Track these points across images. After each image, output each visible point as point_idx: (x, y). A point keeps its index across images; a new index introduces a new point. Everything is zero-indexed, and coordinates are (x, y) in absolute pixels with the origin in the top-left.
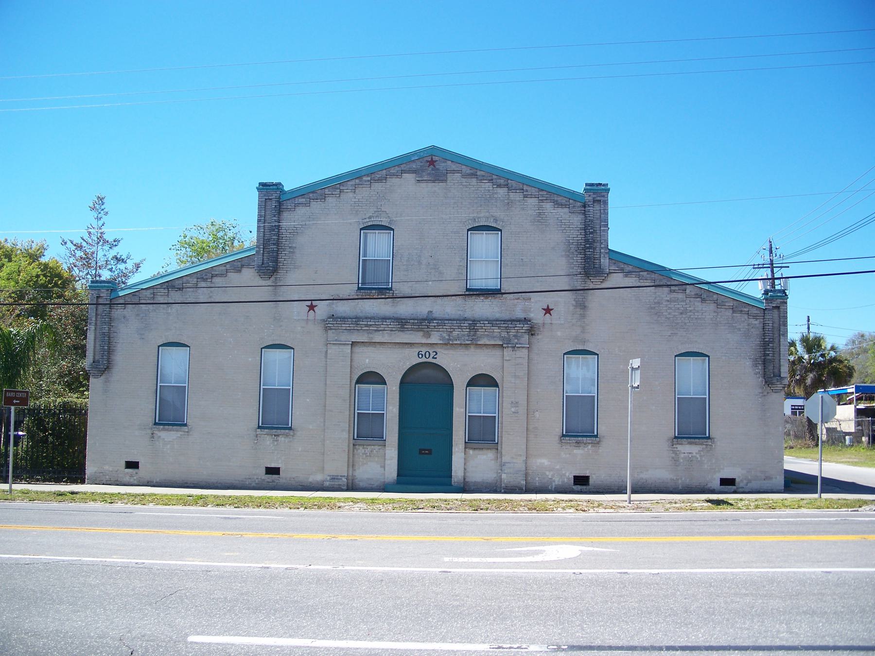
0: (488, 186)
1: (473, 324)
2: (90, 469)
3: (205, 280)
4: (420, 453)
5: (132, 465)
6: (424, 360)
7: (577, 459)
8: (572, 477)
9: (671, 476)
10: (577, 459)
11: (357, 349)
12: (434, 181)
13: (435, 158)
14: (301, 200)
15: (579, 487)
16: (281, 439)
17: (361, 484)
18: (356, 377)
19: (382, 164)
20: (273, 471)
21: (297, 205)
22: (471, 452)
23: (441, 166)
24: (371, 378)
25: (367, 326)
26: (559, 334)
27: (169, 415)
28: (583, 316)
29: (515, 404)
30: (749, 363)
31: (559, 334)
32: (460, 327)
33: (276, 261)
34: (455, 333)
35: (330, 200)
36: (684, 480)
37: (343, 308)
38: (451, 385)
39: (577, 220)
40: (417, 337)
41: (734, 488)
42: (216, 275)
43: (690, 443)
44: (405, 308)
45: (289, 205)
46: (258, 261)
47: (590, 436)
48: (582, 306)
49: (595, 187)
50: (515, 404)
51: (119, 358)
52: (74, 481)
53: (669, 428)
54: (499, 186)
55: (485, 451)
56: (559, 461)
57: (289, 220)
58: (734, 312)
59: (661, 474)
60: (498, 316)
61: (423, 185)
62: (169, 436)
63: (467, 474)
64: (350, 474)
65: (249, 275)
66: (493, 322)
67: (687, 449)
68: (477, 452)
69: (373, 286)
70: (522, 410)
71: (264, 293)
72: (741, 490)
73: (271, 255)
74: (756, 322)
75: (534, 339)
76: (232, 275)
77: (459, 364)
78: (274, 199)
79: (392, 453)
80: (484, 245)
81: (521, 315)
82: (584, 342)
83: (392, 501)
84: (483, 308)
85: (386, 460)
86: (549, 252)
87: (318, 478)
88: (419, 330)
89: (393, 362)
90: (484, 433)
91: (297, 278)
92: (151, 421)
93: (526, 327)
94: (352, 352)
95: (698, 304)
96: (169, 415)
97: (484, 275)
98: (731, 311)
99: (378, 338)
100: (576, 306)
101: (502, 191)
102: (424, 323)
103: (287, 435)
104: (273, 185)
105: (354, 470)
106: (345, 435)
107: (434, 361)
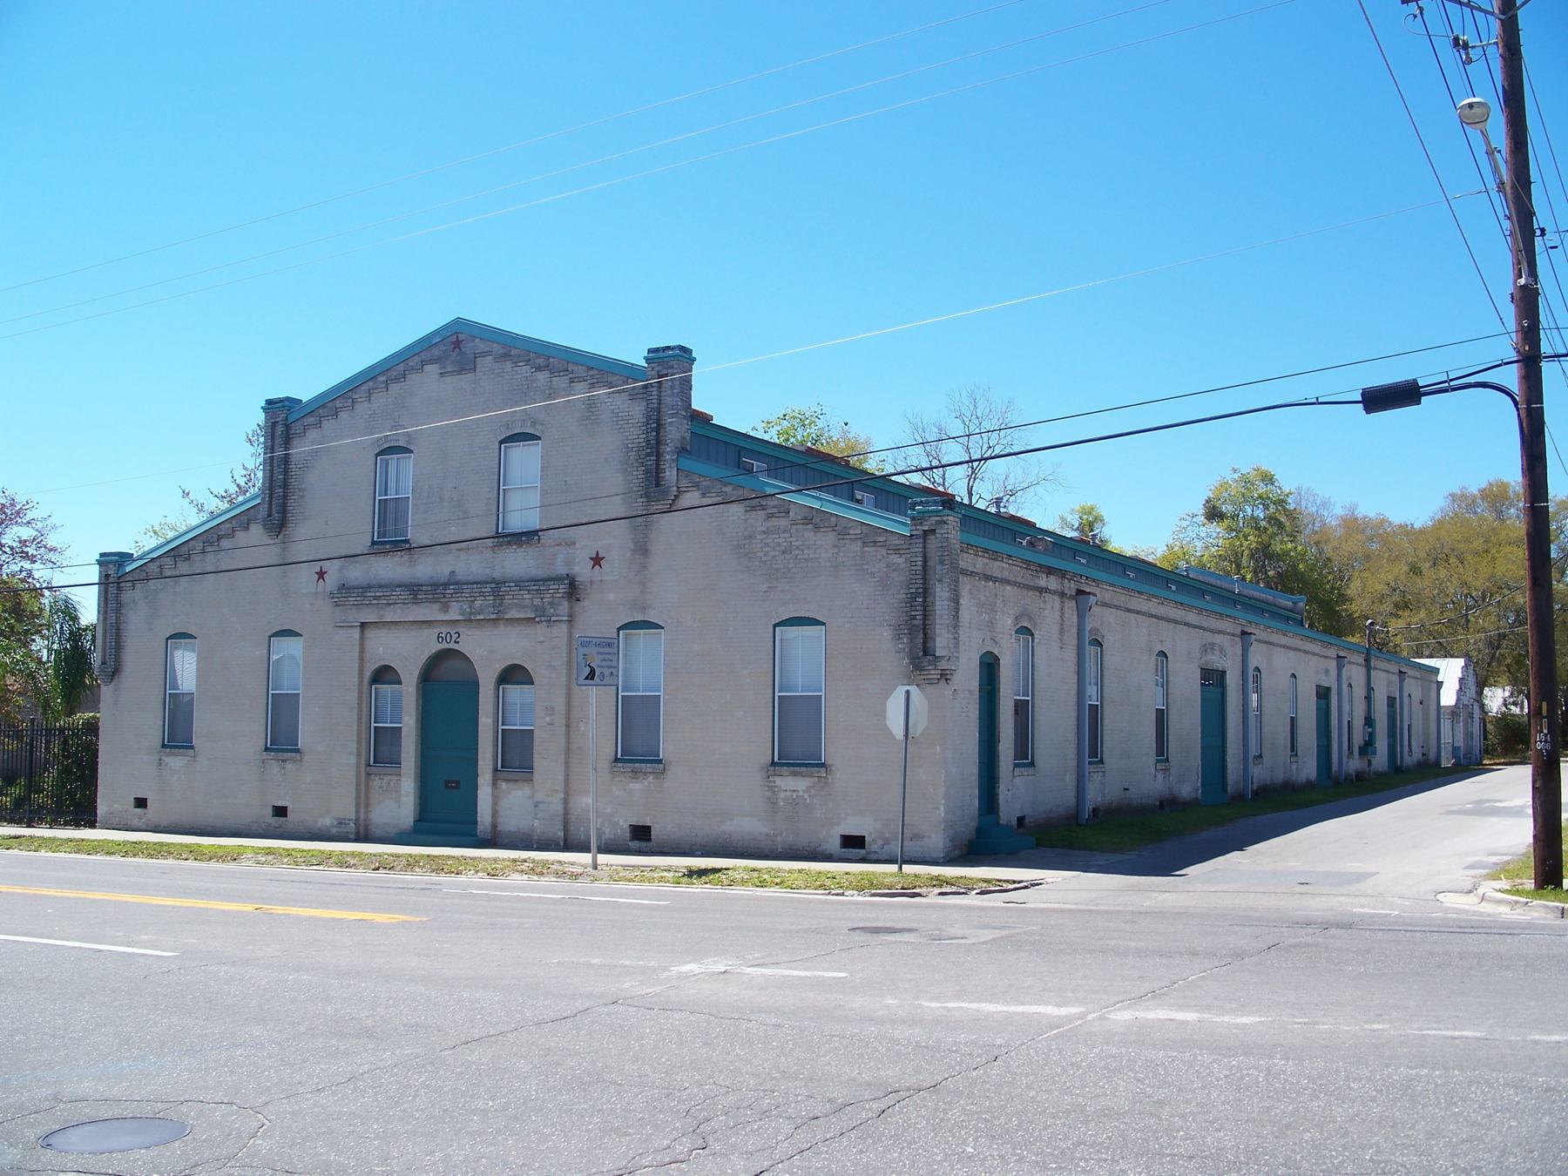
0: (525, 370)
1: (497, 587)
2: (102, 809)
3: (211, 544)
4: (457, 782)
5: (141, 803)
6: (444, 646)
7: (627, 800)
8: (626, 826)
9: (765, 830)
10: (627, 800)
11: (371, 633)
12: (460, 372)
13: (461, 337)
14: (311, 420)
15: (636, 844)
16: (289, 766)
17: (378, 832)
18: (368, 675)
19: (399, 354)
20: (280, 811)
21: (305, 429)
22: (504, 785)
23: (468, 348)
24: (384, 675)
25: (375, 598)
26: (611, 597)
27: (177, 734)
28: (644, 567)
29: (551, 711)
30: (887, 633)
31: (611, 597)
32: (482, 594)
33: (284, 511)
34: (478, 603)
35: (343, 415)
36: (784, 838)
37: (356, 573)
38: (477, 683)
39: (638, 410)
40: (430, 612)
41: (862, 852)
42: (223, 537)
43: (794, 774)
44: (425, 569)
45: (297, 428)
46: (263, 511)
47: (651, 762)
48: (642, 549)
49: (661, 354)
50: (551, 711)
51: (129, 657)
52: (77, 824)
53: (760, 747)
54: (538, 369)
55: (520, 785)
56: (609, 800)
57: (299, 449)
58: (865, 544)
59: (749, 825)
60: (534, 572)
61: (448, 379)
62: (176, 762)
63: (501, 820)
64: (362, 816)
65: (257, 532)
66: (520, 583)
67: (792, 784)
68: (511, 785)
69: (390, 538)
70: (560, 720)
71: (271, 553)
72: (873, 857)
73: (277, 502)
74: (901, 560)
75: (578, 607)
76: (240, 535)
77: (487, 650)
78: (284, 422)
79: (408, 787)
80: (525, 462)
81: (561, 570)
82: (644, 609)
83: (269, 851)
84: (516, 563)
85: (399, 799)
86: (603, 460)
87: (326, 822)
88: (435, 601)
89: (408, 650)
90: (516, 757)
91: (307, 534)
92: (159, 742)
93: (563, 588)
94: (362, 638)
95: (809, 534)
96: (177, 734)
97: (523, 513)
98: (860, 544)
99: (391, 615)
100: (634, 551)
101: (543, 376)
102: (439, 591)
103: (295, 761)
104: (281, 400)
105: (367, 812)
106: (353, 760)
107: (456, 647)
